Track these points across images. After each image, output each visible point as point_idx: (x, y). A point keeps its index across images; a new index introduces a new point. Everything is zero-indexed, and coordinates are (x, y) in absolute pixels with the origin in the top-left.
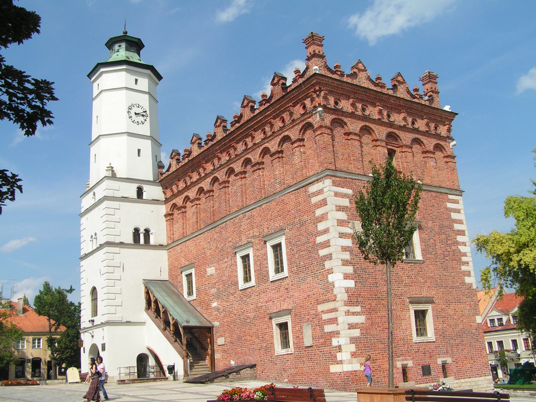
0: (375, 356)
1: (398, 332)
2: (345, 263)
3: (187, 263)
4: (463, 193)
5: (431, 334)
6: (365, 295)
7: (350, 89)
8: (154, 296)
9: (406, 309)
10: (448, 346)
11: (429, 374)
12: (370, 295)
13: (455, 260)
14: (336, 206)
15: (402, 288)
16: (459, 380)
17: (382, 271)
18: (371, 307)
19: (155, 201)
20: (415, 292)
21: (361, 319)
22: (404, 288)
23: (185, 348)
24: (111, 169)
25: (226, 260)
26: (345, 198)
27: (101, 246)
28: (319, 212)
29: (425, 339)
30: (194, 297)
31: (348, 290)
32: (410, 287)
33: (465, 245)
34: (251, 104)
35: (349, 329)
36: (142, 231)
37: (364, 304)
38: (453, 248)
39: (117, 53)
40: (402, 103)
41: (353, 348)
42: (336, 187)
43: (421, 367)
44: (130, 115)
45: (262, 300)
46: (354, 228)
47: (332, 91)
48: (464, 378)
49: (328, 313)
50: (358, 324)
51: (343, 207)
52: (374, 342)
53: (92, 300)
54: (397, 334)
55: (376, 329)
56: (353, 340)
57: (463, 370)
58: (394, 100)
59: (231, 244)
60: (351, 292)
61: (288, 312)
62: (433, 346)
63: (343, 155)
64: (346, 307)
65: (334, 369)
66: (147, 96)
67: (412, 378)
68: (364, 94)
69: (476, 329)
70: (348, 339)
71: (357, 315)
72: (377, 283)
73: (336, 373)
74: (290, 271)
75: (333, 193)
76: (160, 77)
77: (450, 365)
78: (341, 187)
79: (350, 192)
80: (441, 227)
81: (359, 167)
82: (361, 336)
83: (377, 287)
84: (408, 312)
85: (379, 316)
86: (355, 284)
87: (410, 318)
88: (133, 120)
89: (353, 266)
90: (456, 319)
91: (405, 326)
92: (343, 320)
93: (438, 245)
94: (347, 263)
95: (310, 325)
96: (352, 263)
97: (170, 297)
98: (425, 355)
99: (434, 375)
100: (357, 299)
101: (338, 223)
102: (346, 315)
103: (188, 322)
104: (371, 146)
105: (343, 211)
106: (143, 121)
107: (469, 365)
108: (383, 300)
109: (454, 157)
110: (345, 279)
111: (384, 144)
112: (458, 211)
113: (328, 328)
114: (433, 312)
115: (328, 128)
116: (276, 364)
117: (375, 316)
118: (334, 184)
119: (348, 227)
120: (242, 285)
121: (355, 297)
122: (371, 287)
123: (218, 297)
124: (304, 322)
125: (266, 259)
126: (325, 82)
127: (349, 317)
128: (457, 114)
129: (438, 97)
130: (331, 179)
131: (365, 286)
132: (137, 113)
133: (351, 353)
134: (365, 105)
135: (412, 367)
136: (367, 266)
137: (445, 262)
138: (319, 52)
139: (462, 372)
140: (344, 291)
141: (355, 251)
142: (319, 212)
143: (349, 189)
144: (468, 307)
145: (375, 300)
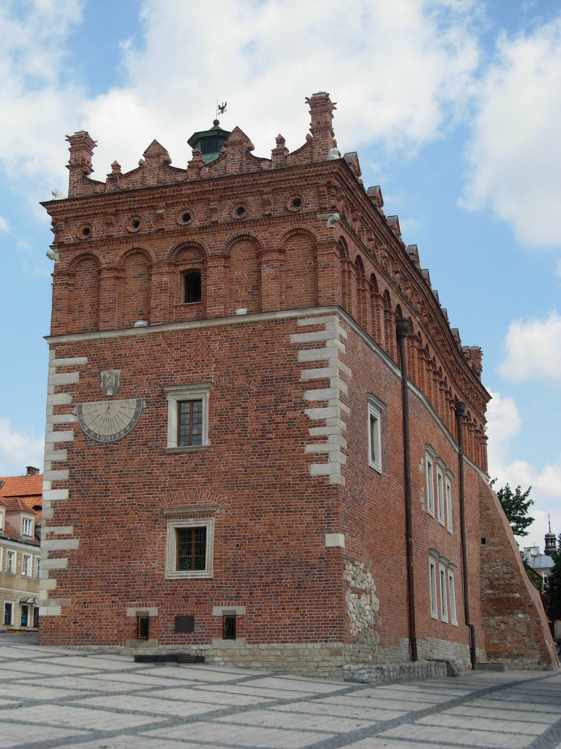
0: (88, 597)
1: (138, 563)
6: (85, 509)
7: (103, 203)
9: (159, 528)
10: (243, 587)
11: (191, 629)
12: (92, 509)
15: (156, 494)
16: (256, 646)
17: (121, 471)
18: (91, 526)
22: (161, 494)
26: (74, 372)
29: (190, 574)
31: (55, 504)
33: (325, 406)
35: (50, 558)
38: (289, 415)
41: (52, 584)
42: (61, 359)
43: (173, 619)
46: (80, 412)
47: (76, 216)
48: (268, 643)
50: (65, 551)
51: (67, 385)
52: (88, 577)
54: (134, 566)
55: (96, 558)
56: (53, 574)
57: (268, 628)
58: (190, 189)
60: (60, 507)
67: (154, 634)
68: (131, 201)
69: (319, 558)
70: (47, 573)
71: (65, 538)
72: (109, 490)
75: (54, 369)
77: (240, 619)
78: (69, 357)
79: (83, 360)
80: (265, 381)
81: (107, 319)
82: (69, 568)
83: (108, 496)
84: (162, 531)
85: (105, 540)
86: (70, 496)
87: (165, 541)
89: (69, 468)
90: (272, 541)
91: (151, 553)
93: (252, 413)
94: (61, 466)
96: (69, 465)
98: (185, 601)
99: (199, 633)
100: (69, 516)
102: (47, 539)
105: (66, 392)
107: (288, 621)
110: (53, 488)
114: (215, 530)
115: (63, 275)
117: (97, 540)
119: (70, 413)
121: (66, 513)
122: (97, 496)
126: (61, 209)
127: (52, 541)
130: (54, 349)
131: (86, 497)
135: (155, 617)
136: (93, 467)
137: (265, 442)
139: (267, 632)
140: (49, 505)
141: (76, 447)
143: (83, 356)
144: (309, 519)
145: (99, 516)
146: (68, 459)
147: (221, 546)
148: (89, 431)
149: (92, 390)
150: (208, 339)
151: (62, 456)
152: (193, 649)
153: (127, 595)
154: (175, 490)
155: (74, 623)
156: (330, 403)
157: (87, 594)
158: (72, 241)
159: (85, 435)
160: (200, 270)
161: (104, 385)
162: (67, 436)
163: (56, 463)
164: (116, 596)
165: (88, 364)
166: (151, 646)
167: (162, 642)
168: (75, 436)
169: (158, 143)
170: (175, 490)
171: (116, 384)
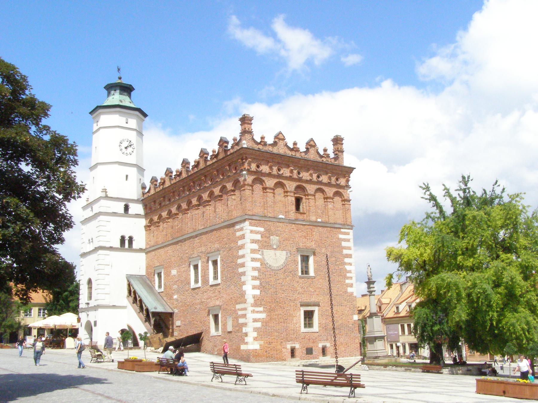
2: (254, 278)
3: (158, 264)
4: (354, 227)
5: (316, 327)
6: (267, 300)
8: (133, 288)
13: (341, 275)
14: (251, 240)
17: (282, 284)
19: (137, 216)
20: (305, 299)
21: (263, 316)
23: (152, 327)
24: (105, 191)
25: (184, 266)
27: (96, 249)
28: (240, 243)
30: (162, 290)
32: (302, 295)
33: (351, 265)
34: (205, 156)
35: (253, 322)
36: (127, 238)
37: (266, 306)
38: (340, 267)
39: (113, 96)
40: (309, 163)
41: (255, 334)
44: (121, 148)
45: (204, 297)
46: (263, 254)
47: (255, 158)
49: (241, 310)
50: (260, 319)
53: (88, 288)
55: (273, 322)
56: (255, 329)
58: (303, 162)
59: (187, 255)
61: (220, 307)
62: (316, 335)
63: (260, 203)
64: (252, 307)
65: (243, 347)
66: (135, 133)
71: (260, 313)
73: (244, 350)
74: (222, 280)
75: (249, 231)
76: (145, 115)
79: (262, 229)
81: (271, 212)
87: (300, 316)
88: (123, 152)
92: (251, 316)
95: (231, 318)
97: (145, 289)
100: (261, 303)
101: (251, 251)
103: (155, 308)
104: (283, 195)
105: (255, 243)
106: (131, 152)
107: (344, 349)
108: (281, 303)
109: (349, 201)
110: (253, 289)
111: (292, 194)
112: (348, 240)
113: (241, 321)
116: (211, 342)
118: (251, 224)
119: (258, 254)
120: (193, 285)
123: (178, 292)
124: (228, 315)
125: (208, 269)
128: (355, 168)
129: (343, 155)
132: (126, 146)
133: (253, 337)
134: (280, 167)
135: (298, 349)
138: (249, 129)
142: (240, 243)
144: (348, 309)
146: (259, 276)
147: (320, 318)
148: (267, 263)
149: (267, 244)
150: (312, 230)
151: (256, 274)
152: (313, 361)
153: (287, 339)
154: (303, 294)
155: (266, 352)
156: (352, 264)
157: (270, 338)
158: (252, 170)
159: (266, 265)
160: (302, 198)
161: (272, 243)
162: (258, 264)
163: (253, 277)
164: (282, 339)
165: (264, 231)
166: (298, 361)
167: (302, 358)
168: (261, 265)
169: (282, 133)
170: (303, 294)
171: (277, 244)
